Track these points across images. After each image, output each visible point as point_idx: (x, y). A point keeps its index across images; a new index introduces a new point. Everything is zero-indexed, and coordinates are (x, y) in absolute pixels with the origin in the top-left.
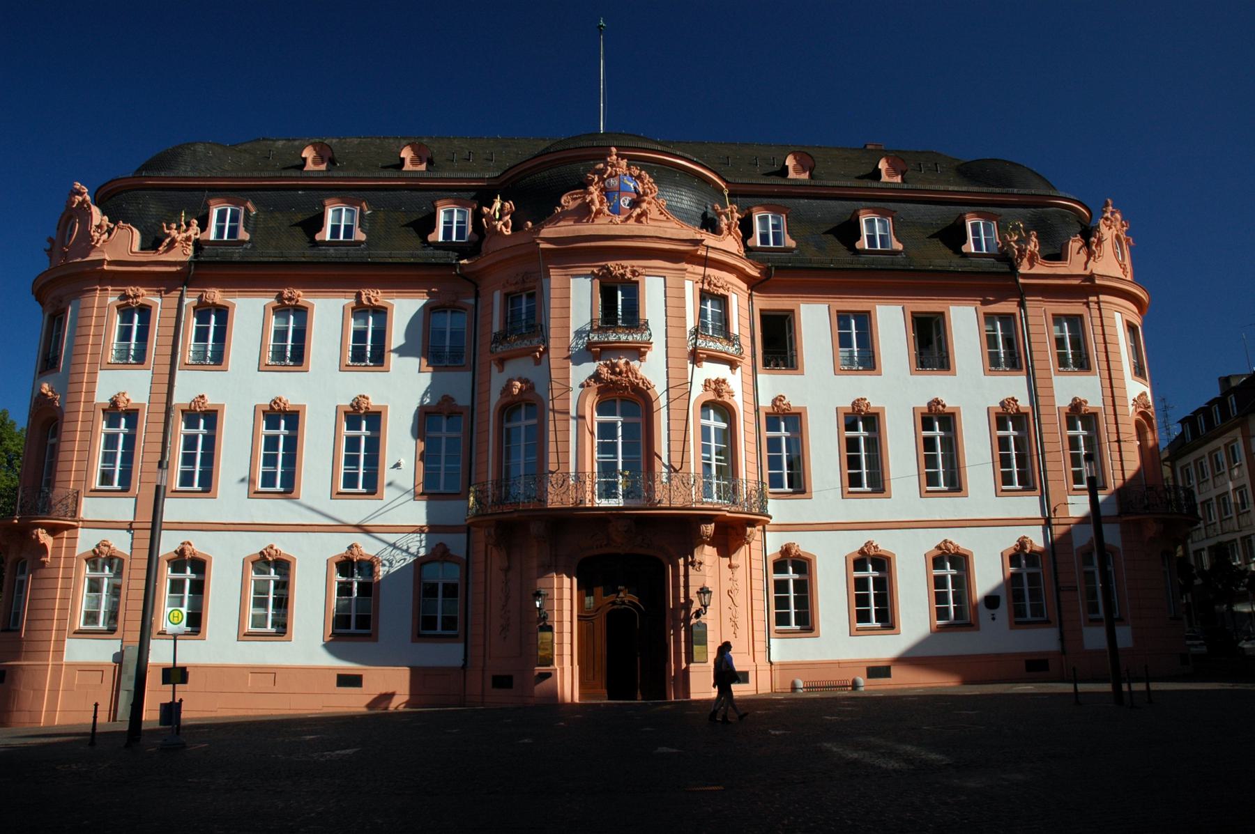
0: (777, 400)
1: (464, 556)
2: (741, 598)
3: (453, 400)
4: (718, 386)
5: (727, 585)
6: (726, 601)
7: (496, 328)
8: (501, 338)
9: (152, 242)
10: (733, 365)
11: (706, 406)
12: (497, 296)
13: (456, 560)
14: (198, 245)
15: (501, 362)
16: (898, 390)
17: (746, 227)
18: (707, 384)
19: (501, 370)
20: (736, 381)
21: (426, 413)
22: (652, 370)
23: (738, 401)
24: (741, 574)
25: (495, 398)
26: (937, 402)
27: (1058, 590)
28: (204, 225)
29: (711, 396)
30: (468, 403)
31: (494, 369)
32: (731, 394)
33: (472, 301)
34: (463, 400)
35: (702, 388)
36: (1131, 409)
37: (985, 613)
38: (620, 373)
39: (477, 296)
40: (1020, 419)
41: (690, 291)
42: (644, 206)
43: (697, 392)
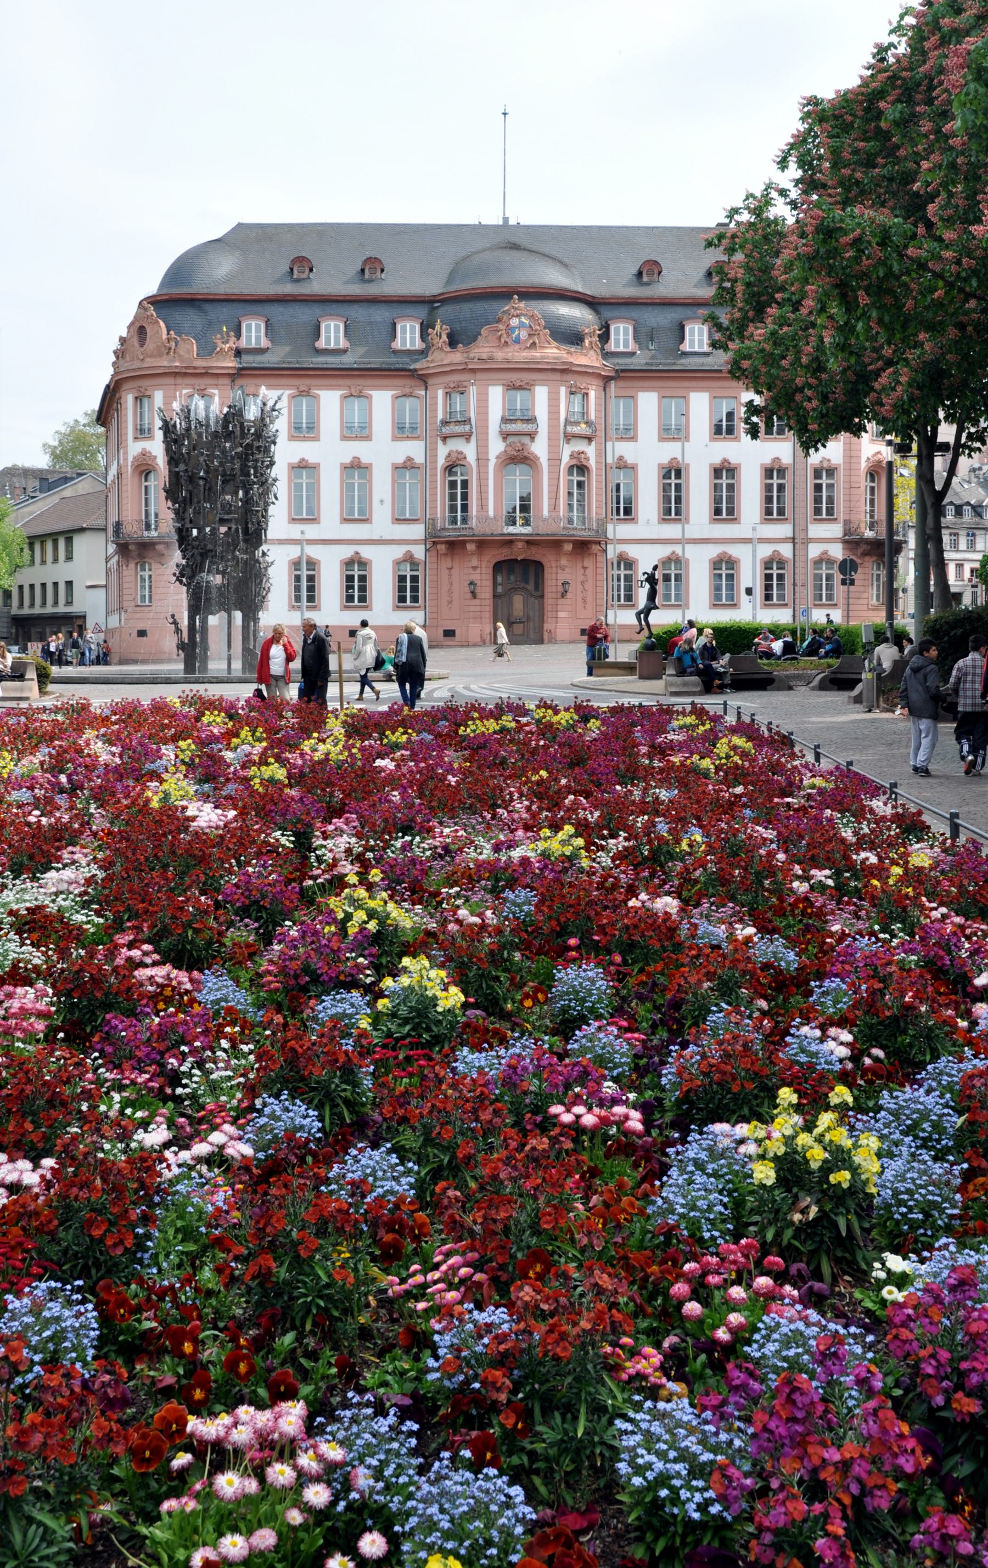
0: (621, 458)
2: (589, 586)
5: (581, 578)
6: (580, 587)
7: (440, 416)
8: (445, 423)
9: (207, 349)
10: (589, 439)
11: (570, 469)
12: (440, 393)
14: (238, 353)
15: (445, 439)
16: (701, 453)
17: (605, 337)
18: (572, 456)
20: (590, 451)
22: (540, 448)
23: (592, 463)
24: (589, 572)
25: (441, 461)
26: (725, 460)
27: (794, 585)
28: (238, 336)
29: (574, 462)
31: (440, 442)
32: (587, 459)
34: (419, 459)
36: (864, 465)
37: (744, 597)
40: (782, 472)
41: (563, 391)
43: (566, 459)
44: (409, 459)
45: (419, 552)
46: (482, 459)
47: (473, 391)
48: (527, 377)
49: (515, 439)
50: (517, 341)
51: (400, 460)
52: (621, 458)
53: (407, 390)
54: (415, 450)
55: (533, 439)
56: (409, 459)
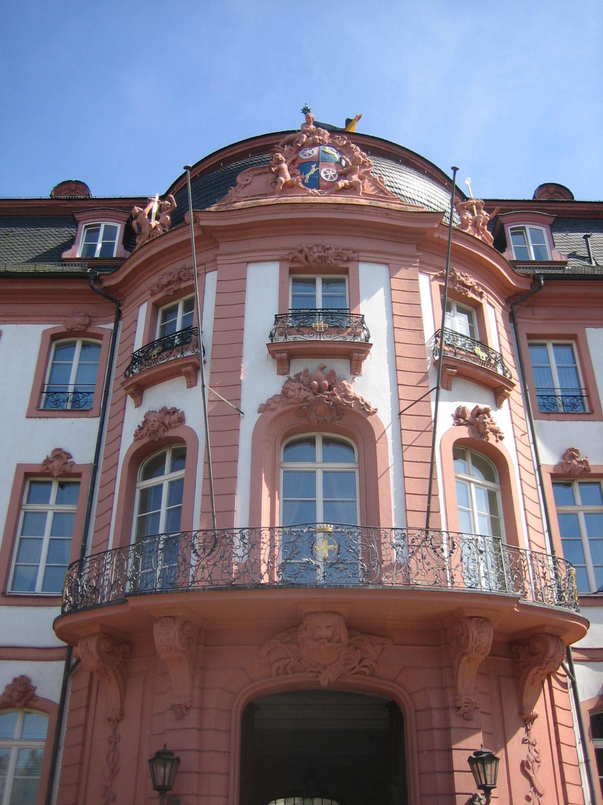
0: (571, 454)
1: (57, 699)
3: (69, 456)
4: (476, 422)
12: (143, 312)
13: (43, 706)
18: (459, 416)
19: (138, 404)
21: (27, 475)
30: (90, 459)
33: (111, 326)
34: (83, 456)
35: (451, 421)
38: (320, 390)
39: (118, 317)
42: (355, 178)
44: (60, 455)
45: (48, 678)
46: (224, 419)
47: (211, 279)
48: (336, 242)
49: (312, 365)
50: (315, 182)
51: (37, 456)
52: (571, 454)
53: (77, 321)
54: (76, 437)
55: (356, 370)
56: (60, 455)
